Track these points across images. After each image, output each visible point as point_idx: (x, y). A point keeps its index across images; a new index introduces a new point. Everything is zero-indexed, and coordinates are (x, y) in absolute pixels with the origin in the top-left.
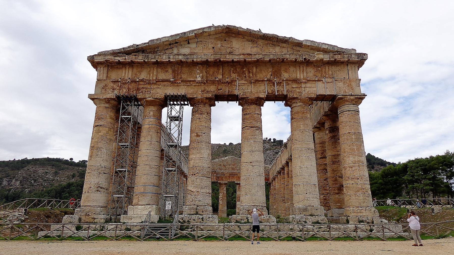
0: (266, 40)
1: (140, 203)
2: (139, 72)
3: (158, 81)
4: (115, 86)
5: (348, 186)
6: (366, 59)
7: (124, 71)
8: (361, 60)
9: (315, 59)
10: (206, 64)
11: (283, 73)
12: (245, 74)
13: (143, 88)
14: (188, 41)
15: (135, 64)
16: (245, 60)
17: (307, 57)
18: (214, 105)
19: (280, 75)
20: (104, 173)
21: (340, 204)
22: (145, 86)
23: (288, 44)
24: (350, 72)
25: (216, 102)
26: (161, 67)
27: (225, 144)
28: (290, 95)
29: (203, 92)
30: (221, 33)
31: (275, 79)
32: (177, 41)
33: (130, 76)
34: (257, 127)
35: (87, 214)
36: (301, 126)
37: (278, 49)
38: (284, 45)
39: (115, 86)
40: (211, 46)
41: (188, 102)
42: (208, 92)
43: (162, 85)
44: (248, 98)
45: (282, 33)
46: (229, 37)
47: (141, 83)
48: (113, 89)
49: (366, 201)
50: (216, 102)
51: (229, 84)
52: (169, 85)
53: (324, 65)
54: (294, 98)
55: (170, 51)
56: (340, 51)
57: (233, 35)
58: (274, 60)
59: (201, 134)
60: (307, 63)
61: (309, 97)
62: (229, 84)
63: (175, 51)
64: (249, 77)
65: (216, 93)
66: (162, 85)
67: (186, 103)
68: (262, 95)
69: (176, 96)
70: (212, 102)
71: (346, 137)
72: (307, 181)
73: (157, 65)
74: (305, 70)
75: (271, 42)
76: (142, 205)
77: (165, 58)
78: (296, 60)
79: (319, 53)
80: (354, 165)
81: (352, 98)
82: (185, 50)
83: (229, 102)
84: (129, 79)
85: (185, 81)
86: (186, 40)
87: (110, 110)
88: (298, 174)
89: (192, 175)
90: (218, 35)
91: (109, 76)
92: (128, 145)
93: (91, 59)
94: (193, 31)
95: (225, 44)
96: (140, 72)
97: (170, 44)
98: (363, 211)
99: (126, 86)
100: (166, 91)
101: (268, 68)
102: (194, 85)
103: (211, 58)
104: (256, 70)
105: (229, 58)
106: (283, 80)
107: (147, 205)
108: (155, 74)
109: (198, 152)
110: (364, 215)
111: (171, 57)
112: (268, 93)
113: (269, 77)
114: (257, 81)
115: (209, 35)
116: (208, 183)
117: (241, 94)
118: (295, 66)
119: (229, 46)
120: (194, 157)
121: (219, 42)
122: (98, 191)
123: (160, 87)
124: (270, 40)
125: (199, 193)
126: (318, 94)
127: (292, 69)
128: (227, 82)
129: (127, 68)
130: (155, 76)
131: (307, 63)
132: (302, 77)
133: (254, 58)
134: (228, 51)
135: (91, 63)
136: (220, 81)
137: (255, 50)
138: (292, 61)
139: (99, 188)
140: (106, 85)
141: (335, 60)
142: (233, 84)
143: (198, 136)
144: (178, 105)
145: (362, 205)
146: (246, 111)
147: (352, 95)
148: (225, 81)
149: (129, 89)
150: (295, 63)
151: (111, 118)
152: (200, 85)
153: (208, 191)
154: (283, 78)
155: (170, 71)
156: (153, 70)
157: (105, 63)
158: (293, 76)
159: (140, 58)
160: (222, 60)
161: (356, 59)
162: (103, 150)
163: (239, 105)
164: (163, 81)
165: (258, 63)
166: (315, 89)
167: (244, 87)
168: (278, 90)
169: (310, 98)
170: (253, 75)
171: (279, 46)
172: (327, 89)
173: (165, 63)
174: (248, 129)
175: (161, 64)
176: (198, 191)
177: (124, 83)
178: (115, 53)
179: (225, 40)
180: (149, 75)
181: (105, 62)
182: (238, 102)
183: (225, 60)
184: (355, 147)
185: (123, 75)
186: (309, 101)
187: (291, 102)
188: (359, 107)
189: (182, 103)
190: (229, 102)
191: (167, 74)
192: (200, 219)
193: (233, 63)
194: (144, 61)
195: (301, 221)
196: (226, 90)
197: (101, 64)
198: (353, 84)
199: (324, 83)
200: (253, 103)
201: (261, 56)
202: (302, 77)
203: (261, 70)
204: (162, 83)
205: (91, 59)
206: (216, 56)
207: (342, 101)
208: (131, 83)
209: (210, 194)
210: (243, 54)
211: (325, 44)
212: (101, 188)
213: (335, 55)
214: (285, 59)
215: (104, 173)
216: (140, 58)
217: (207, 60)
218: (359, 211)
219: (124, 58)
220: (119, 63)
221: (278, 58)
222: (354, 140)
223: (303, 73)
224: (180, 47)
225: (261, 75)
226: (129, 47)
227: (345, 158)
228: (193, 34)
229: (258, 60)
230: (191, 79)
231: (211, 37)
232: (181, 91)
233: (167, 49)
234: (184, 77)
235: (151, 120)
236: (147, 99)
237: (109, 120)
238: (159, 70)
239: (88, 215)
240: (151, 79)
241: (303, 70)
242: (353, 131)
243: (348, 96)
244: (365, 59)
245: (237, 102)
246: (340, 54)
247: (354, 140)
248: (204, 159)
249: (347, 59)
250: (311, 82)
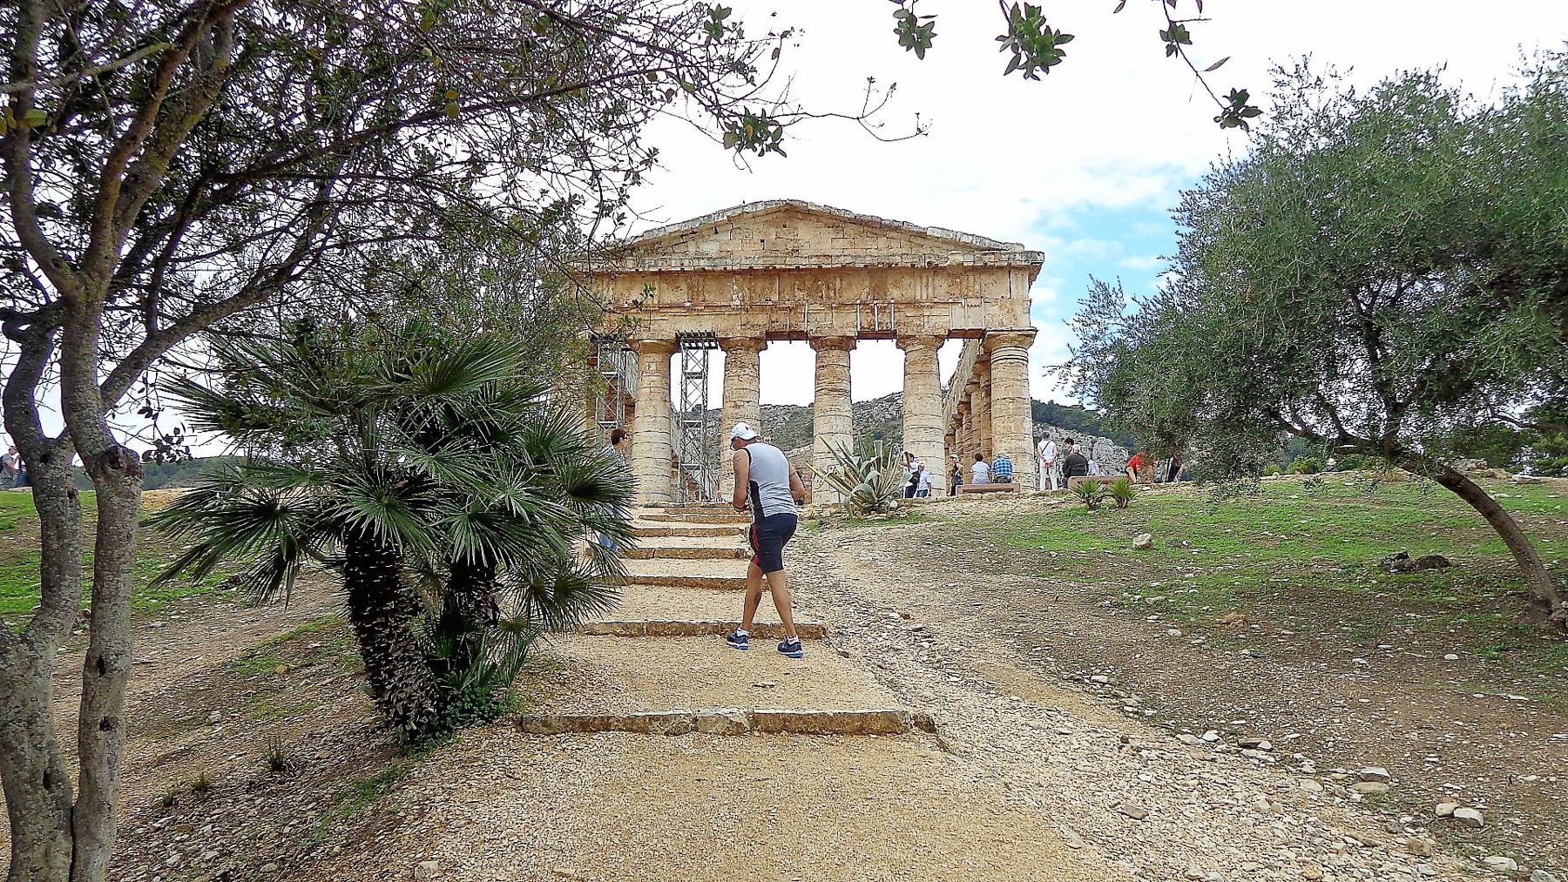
9: (948, 263)
10: (750, 273)
25: (769, 343)
28: (901, 331)
31: (875, 302)
37: (882, 242)
38: (895, 235)
40: (757, 237)
45: (887, 213)
46: (791, 218)
50: (769, 343)
51: (791, 311)
55: (682, 248)
56: (993, 249)
57: (800, 216)
60: (935, 270)
62: (791, 311)
63: (692, 248)
64: (829, 298)
67: (713, 344)
68: (852, 333)
69: (696, 335)
70: (762, 345)
77: (674, 265)
81: (1012, 334)
82: (710, 247)
92: (615, 424)
94: (724, 211)
95: (783, 232)
97: (682, 236)
100: (678, 327)
103: (759, 265)
104: (842, 284)
105: (792, 262)
111: (686, 263)
113: (863, 297)
118: (912, 276)
121: (773, 230)
127: (907, 281)
131: (935, 270)
147: (1011, 330)
148: (784, 306)
155: (684, 286)
165: (844, 271)
166: (947, 319)
167: (818, 317)
171: (884, 236)
179: (785, 226)
183: (783, 267)
188: (1029, 351)
189: (707, 344)
191: (678, 293)
196: (783, 321)
198: (1019, 309)
201: (849, 260)
202: (925, 297)
213: (985, 254)
225: (850, 293)
228: (725, 218)
229: (843, 267)
230: (723, 304)
231: (758, 220)
232: (705, 324)
234: (710, 298)
235: (654, 378)
236: (646, 341)
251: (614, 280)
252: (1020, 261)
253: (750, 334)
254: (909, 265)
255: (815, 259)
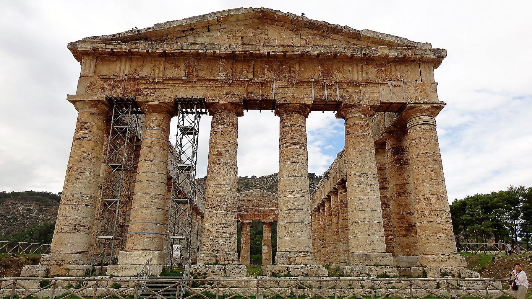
0: (313, 29)
1: (136, 247)
2: (140, 67)
3: (165, 79)
4: (106, 85)
5: (424, 225)
6: (445, 57)
7: (119, 65)
8: (438, 57)
9: (379, 54)
10: (232, 57)
11: (335, 73)
12: (285, 73)
13: (144, 88)
14: (208, 28)
15: (134, 55)
16: (285, 55)
17: (367, 51)
18: (242, 115)
19: (332, 76)
20: (86, 205)
21: (408, 250)
22: (148, 86)
23: (342, 35)
24: (423, 74)
25: (245, 111)
26: (170, 61)
27: (247, 177)
29: (228, 95)
30: (252, 18)
32: (193, 27)
33: (127, 72)
34: (301, 143)
35: (58, 263)
36: (361, 143)
37: (327, 42)
38: (336, 36)
39: (106, 85)
40: (238, 35)
41: (207, 110)
42: (234, 95)
43: (171, 85)
44: (289, 104)
45: (333, 20)
46: (263, 23)
47: (143, 81)
48: (103, 89)
49: (449, 246)
50: (245, 111)
51: (262, 85)
52: (181, 85)
53: (389, 63)
54: (351, 106)
55: (183, 40)
56: (411, 46)
57: (269, 22)
58: (324, 54)
59: (224, 152)
60: (368, 60)
61: (370, 104)
62: (262, 85)
63: (190, 40)
65: (245, 97)
66: (171, 85)
67: (204, 110)
69: (190, 100)
71: (419, 159)
72: (369, 217)
73: (166, 58)
74: (364, 69)
75: (320, 32)
76: (139, 250)
77: (176, 49)
78: (353, 55)
79: (383, 47)
80: (431, 196)
81: (427, 107)
83: (261, 111)
84: (126, 75)
85: (203, 80)
86: (206, 27)
87: (97, 117)
88: (357, 208)
89: (211, 208)
90: (249, 20)
91: (98, 71)
92: (121, 166)
93: (73, 47)
94: (215, 13)
95: (259, 34)
96: (142, 67)
97: (183, 31)
98: (446, 260)
99: (121, 85)
100: (176, 94)
101: (315, 66)
102: (215, 85)
103: (239, 51)
104: (300, 68)
105: (263, 50)
106: (336, 82)
107: (146, 250)
108: (161, 69)
109: (219, 176)
110: (447, 265)
111: (185, 47)
112: (316, 99)
113: (316, 77)
114: (301, 82)
115: (236, 21)
116: (233, 219)
117: (279, 98)
118: (351, 64)
119: (263, 36)
120: (214, 183)
121: (250, 30)
122: (75, 230)
123: (168, 87)
124: (319, 30)
125: (219, 234)
126: (382, 101)
127: (347, 68)
128: (261, 82)
129: (123, 61)
130: (162, 73)
131: (368, 60)
132: (360, 78)
133: (297, 52)
134: (262, 41)
135: (73, 53)
136: (250, 81)
137: (297, 42)
138: (347, 57)
139: (77, 226)
140: (93, 84)
141: (405, 56)
142: (268, 85)
143: (219, 154)
144: (192, 113)
145: (445, 251)
146: (286, 122)
147: (427, 104)
149: (125, 89)
150: (352, 60)
151: (98, 128)
152: (223, 85)
153: (232, 231)
154: (334, 78)
155: (183, 66)
156: (160, 64)
157: (93, 54)
158: (349, 77)
159: (141, 48)
160: (254, 52)
161: (432, 57)
162: (85, 172)
163: (275, 115)
164: (173, 79)
165: (302, 58)
166: (378, 94)
167: (282, 90)
168: (329, 94)
169: (371, 106)
170: (295, 74)
171: (329, 37)
172: (394, 96)
173: (177, 56)
174: (288, 146)
175: (170, 56)
176: (218, 230)
177: (118, 81)
178: (106, 40)
179: (258, 28)
180: (153, 71)
181: (92, 52)
182: (274, 111)
183: (258, 52)
184: (433, 173)
185: (118, 70)
186: (370, 110)
187: (346, 111)
189: (199, 110)
190: (261, 111)
191: (179, 71)
192: (221, 270)
193: (268, 58)
194: (147, 51)
195: (362, 274)
196: (258, 94)
197: (87, 55)
198: (429, 90)
199: (390, 87)
200: (296, 111)
201: (306, 49)
202: (360, 78)
203: (306, 69)
204: (171, 82)
205: (73, 47)
206: (245, 48)
207: (413, 111)
208: (128, 81)
209: (235, 234)
210: (283, 46)
211: (391, 36)
212: (81, 226)
214: (338, 53)
215: (86, 205)
216: (141, 48)
217: (234, 52)
218: (440, 259)
219: (119, 46)
220: (112, 53)
221: (329, 52)
222: (430, 163)
223: (362, 74)
224: (197, 35)
225: (306, 74)
226: (126, 32)
227: (418, 187)
228: (216, 18)
229: (302, 55)
230: (211, 78)
231: (239, 23)
232: (198, 93)
233: (179, 37)
234: (202, 74)
235: (155, 131)
236: (150, 103)
237: (96, 131)
238: (168, 65)
239: (60, 265)
240: (156, 76)
241: (362, 70)
242: (429, 151)
243: (423, 105)
244: (443, 57)
245: (272, 111)
246: (410, 49)
247: (430, 163)
248: (227, 186)
249: (420, 56)
250: (373, 85)
251: (131, 60)
252: (429, 55)
253: (231, 100)
254: (350, 55)
255: (281, 48)
